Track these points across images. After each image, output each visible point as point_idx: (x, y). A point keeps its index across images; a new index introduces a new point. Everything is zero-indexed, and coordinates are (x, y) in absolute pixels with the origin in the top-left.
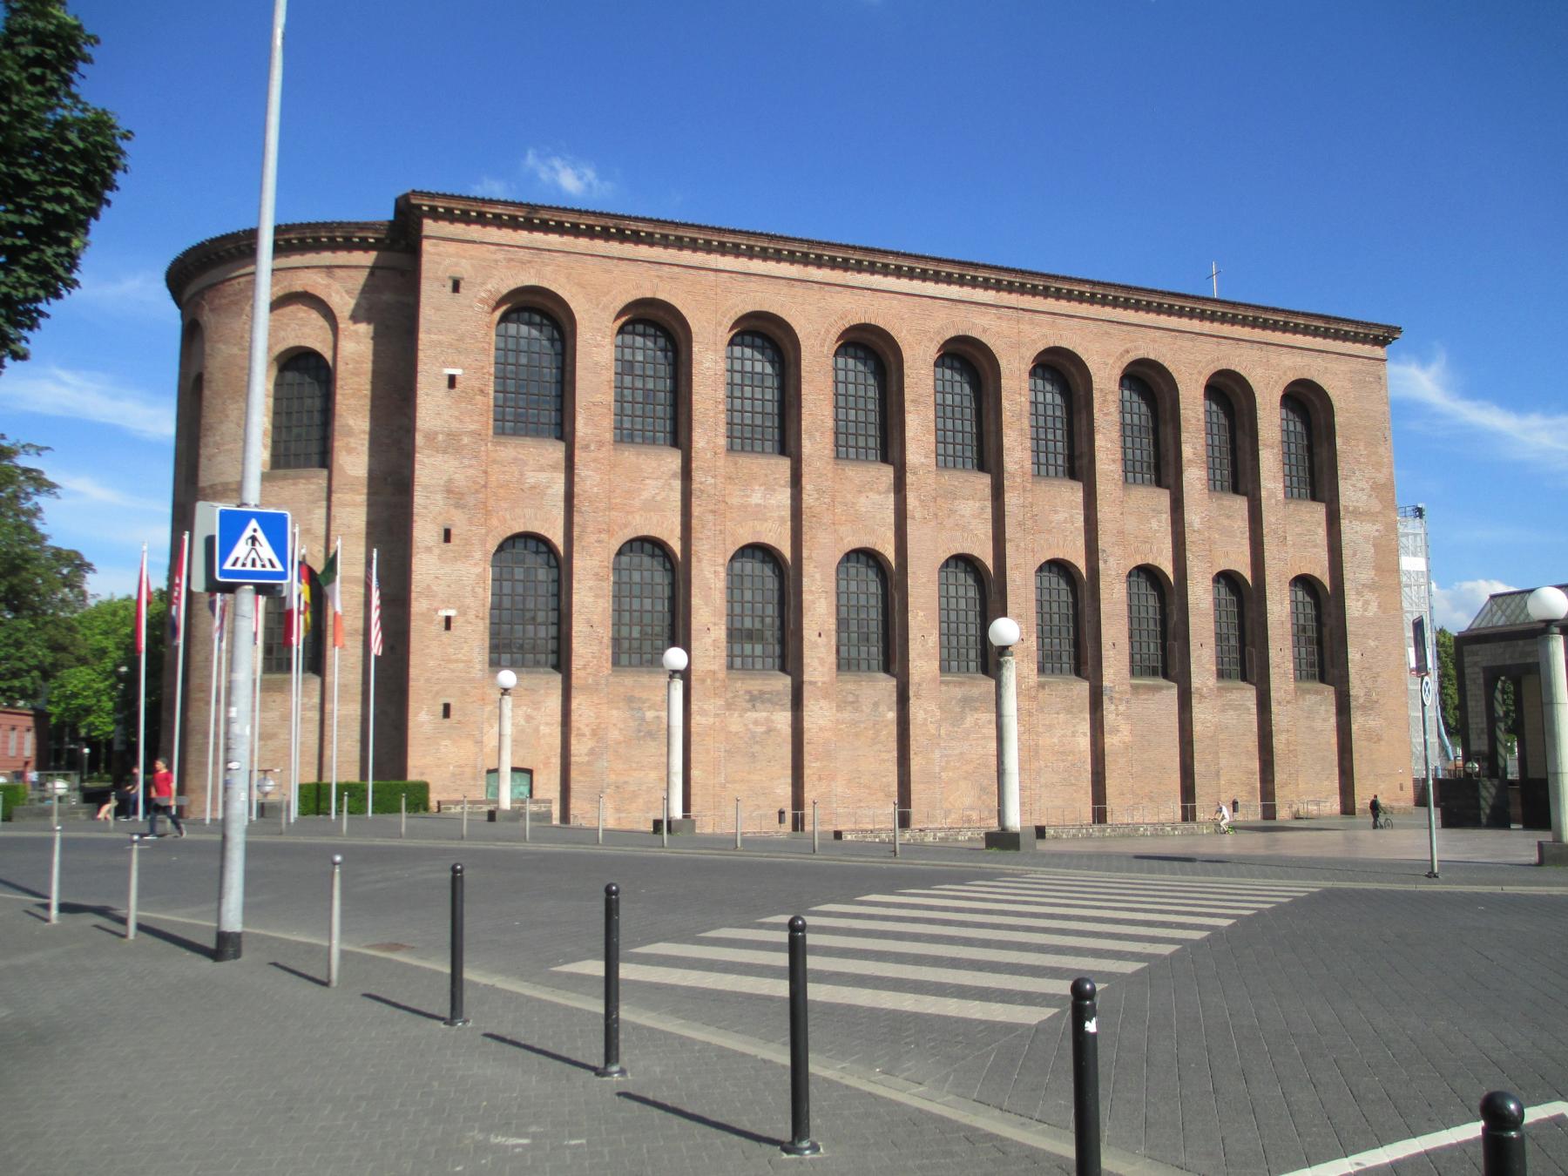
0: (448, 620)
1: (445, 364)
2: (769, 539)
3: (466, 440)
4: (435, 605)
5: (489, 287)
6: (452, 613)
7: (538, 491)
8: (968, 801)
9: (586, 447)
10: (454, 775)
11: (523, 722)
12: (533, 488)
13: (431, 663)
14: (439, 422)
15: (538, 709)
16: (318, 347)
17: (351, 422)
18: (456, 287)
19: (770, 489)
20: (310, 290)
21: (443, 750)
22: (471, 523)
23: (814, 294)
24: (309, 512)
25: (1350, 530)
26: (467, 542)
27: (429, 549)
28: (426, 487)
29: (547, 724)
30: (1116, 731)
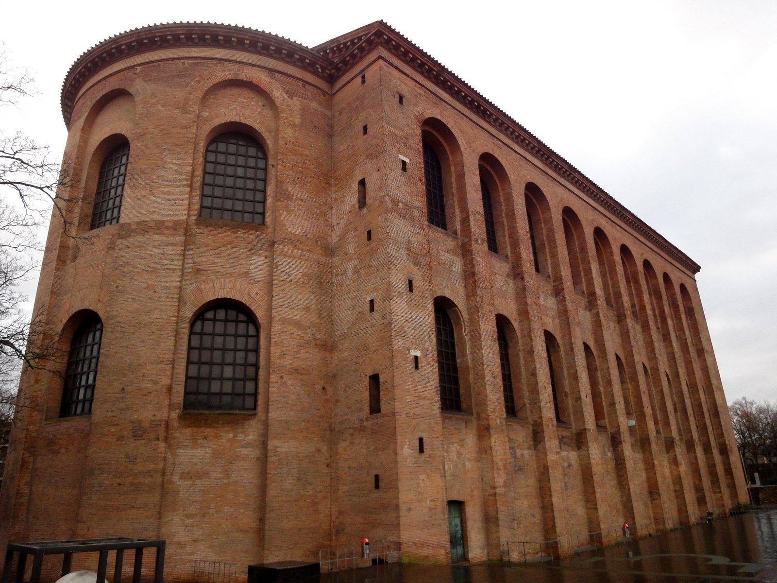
0: (416, 358)
3: (416, 213)
4: (408, 344)
5: (418, 109)
6: (418, 353)
9: (476, 241)
10: (430, 509)
11: (455, 458)
12: (444, 264)
13: (409, 398)
14: (398, 193)
15: (462, 446)
16: (257, 126)
17: (290, 189)
20: (255, 81)
21: (422, 485)
22: (424, 280)
27: (400, 295)
29: (470, 460)
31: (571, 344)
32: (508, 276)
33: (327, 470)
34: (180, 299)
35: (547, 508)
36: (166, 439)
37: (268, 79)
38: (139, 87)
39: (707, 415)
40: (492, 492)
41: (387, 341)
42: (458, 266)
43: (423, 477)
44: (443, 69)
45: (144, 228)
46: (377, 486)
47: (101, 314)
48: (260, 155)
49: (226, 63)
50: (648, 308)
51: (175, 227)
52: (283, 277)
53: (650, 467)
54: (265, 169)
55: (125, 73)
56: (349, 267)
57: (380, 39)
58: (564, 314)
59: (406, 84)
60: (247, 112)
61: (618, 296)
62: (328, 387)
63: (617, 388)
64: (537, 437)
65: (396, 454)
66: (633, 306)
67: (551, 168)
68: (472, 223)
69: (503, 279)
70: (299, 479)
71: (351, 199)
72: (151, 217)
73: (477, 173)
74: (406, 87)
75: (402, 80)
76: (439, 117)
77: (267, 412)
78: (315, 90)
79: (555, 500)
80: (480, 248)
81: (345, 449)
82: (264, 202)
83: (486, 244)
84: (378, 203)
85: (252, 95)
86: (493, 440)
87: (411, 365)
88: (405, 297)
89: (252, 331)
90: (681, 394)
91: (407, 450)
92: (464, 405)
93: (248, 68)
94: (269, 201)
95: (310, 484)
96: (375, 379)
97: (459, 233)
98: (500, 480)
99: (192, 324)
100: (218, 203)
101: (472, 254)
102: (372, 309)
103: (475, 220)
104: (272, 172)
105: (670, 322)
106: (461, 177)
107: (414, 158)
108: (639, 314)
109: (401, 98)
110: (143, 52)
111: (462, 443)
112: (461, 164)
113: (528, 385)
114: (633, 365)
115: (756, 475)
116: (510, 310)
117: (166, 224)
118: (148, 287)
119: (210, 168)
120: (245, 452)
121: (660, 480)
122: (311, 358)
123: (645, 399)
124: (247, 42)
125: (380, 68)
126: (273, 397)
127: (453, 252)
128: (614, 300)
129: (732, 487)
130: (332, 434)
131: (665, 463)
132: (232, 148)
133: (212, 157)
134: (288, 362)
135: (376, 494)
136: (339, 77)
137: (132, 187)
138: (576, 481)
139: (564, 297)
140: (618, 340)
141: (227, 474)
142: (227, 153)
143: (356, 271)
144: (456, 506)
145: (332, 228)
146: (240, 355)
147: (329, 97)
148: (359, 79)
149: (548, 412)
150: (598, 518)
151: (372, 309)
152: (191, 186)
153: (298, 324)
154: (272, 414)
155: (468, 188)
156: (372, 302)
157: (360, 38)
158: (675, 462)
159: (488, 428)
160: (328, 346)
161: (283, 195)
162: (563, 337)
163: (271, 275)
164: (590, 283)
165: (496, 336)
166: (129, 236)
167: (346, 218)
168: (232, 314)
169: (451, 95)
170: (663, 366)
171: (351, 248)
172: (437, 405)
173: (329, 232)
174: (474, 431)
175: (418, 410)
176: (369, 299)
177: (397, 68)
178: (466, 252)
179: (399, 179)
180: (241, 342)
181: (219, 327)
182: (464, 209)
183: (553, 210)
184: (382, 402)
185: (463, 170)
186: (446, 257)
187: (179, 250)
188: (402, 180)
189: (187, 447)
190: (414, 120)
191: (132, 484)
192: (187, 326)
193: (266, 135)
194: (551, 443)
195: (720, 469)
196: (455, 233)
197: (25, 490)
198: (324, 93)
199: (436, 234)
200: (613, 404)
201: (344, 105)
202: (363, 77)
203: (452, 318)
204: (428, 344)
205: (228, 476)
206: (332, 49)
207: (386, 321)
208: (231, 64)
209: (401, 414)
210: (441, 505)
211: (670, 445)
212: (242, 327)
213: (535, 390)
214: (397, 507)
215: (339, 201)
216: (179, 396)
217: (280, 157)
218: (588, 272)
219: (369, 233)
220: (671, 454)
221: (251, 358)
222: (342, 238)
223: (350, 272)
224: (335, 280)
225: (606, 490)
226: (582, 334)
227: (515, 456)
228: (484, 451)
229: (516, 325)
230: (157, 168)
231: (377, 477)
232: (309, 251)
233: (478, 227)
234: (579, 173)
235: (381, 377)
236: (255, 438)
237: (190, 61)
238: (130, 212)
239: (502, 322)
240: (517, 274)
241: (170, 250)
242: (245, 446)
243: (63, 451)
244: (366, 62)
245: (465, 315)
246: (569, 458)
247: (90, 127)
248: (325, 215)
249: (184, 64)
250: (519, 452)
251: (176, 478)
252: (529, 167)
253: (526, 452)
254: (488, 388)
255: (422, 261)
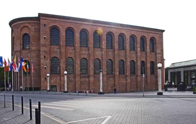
0: (45, 67)
2: (85, 57)
7: (56, 52)
8: (110, 89)
18: (45, 26)
19: (85, 51)
25: (158, 55)
26: (47, 58)
30: (128, 80)
87: (43, 69)
152: (20, 45)
153: (34, 63)
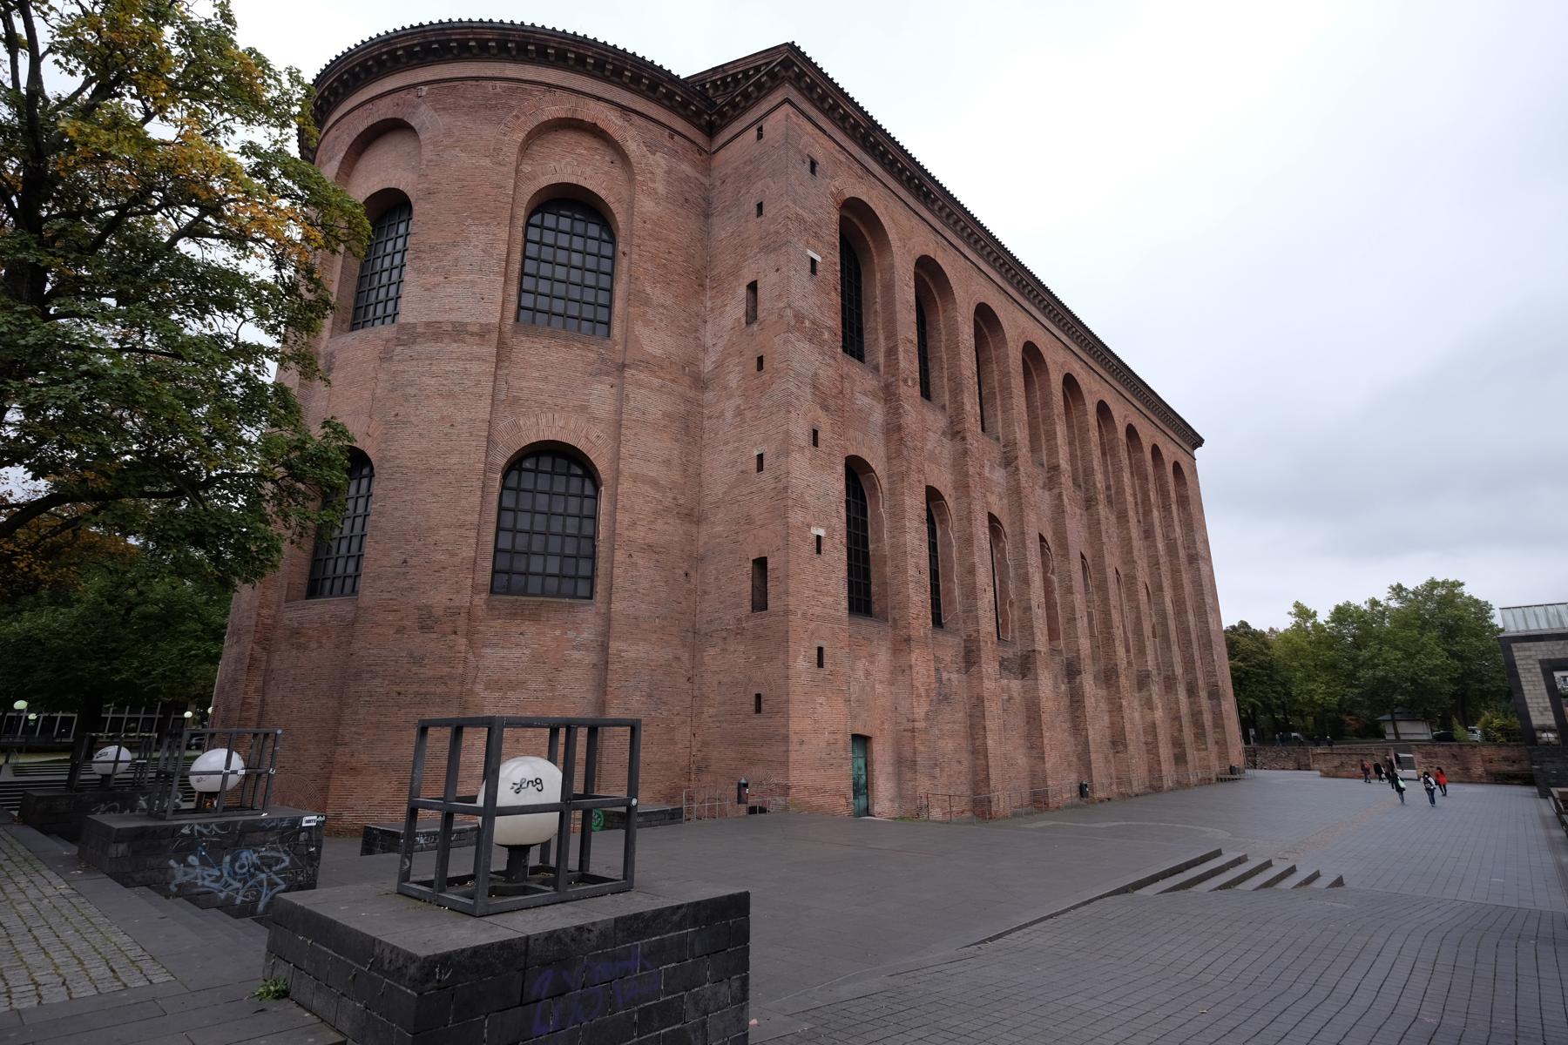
0: (819, 537)
1: (808, 245)
3: (826, 335)
4: (809, 519)
6: (822, 532)
9: (905, 381)
16: (602, 193)
17: (648, 290)
20: (601, 124)
21: (820, 710)
23: (1012, 307)
24: (585, 385)
28: (798, 374)
31: (1023, 533)
32: (944, 433)
33: (688, 685)
34: (490, 440)
35: (978, 752)
36: (469, 635)
37: (619, 122)
38: (423, 117)
39: (1195, 645)
40: (909, 726)
41: (781, 515)
42: (878, 415)
43: (821, 700)
44: (875, 126)
45: (435, 332)
46: (758, 710)
47: (371, 453)
48: (605, 237)
49: (558, 92)
50: (1128, 491)
51: (483, 333)
52: (636, 416)
53: (1116, 708)
54: (612, 258)
55: (402, 94)
56: (729, 407)
57: (786, 71)
58: (1015, 493)
59: (822, 146)
60: (589, 171)
61: (1088, 472)
62: (692, 573)
63: (1078, 598)
64: (970, 657)
65: (788, 667)
66: (1108, 488)
67: (1011, 284)
68: (901, 355)
69: (937, 437)
70: (650, 696)
71: (736, 309)
72: (446, 317)
73: (912, 283)
74: (821, 149)
75: (821, 143)
76: (865, 198)
77: (610, 602)
78: (687, 144)
79: (989, 742)
80: (910, 392)
81: (714, 658)
82: (609, 307)
83: (918, 388)
84: (775, 318)
85: (595, 144)
86: (914, 656)
88: (807, 453)
89: (589, 490)
90: (1164, 616)
91: (802, 663)
92: (875, 608)
93: (592, 103)
94: (618, 305)
95: (665, 703)
96: (761, 564)
97: (882, 368)
98: (921, 710)
99: (505, 477)
100: (543, 303)
101: (898, 400)
102: (760, 468)
103: (906, 351)
104: (623, 264)
105: (1155, 514)
106: (889, 288)
107: (827, 255)
108: (1115, 500)
109: (813, 164)
110: (432, 63)
111: (872, 657)
112: (892, 267)
113: (962, 585)
114: (1101, 570)
115: (1252, 732)
116: (944, 481)
117: (469, 328)
118: (443, 418)
119: (532, 250)
120: (577, 655)
121: (1128, 726)
122: (670, 531)
123: (1115, 615)
124: (591, 61)
125: (782, 119)
126: (618, 582)
127: (874, 396)
128: (1083, 479)
129: (1222, 744)
130: (695, 636)
131: (1136, 704)
132: (565, 223)
133: (534, 234)
134: (639, 534)
135: (757, 720)
136: (722, 127)
137: (418, 271)
138: (1018, 721)
139: (1017, 469)
140: (1084, 534)
141: (551, 683)
142: (557, 230)
143: (739, 413)
144: (861, 741)
145: (705, 350)
146: (572, 525)
147: (706, 157)
148: (753, 132)
149: (987, 626)
150: (1044, 771)
151: (760, 468)
153: (655, 483)
154: (617, 606)
155: (898, 306)
156: (760, 457)
157: (757, 69)
158: (1149, 704)
159: (908, 640)
160: (693, 517)
161: (638, 298)
162: (1012, 524)
163: (619, 412)
164: (1053, 451)
165: (924, 515)
166: (414, 342)
167: (726, 337)
168: (561, 463)
169: (883, 165)
170: (1142, 575)
171: (733, 380)
172: (845, 604)
173: (701, 356)
174: (889, 644)
175: (818, 610)
176: (756, 453)
177: (809, 119)
178: (889, 395)
179: (803, 287)
180: (574, 505)
181: (543, 482)
182: (891, 335)
183: (1011, 344)
184: (770, 597)
185: (892, 279)
186: (863, 401)
187: (489, 367)
188: (810, 286)
189: (496, 645)
190: (831, 200)
191: (417, 694)
192: (499, 476)
193: (614, 207)
194: (989, 667)
195: (1207, 718)
196: (876, 368)
197: (255, 699)
198: (701, 151)
199: (852, 367)
200: (1072, 620)
201: (729, 171)
202: (760, 129)
203: (865, 485)
204: (835, 520)
205: (553, 688)
206: (714, 83)
207: (780, 486)
208: (565, 94)
209: (795, 614)
210: (844, 740)
211: (1142, 681)
212: (575, 483)
213: (971, 593)
214: (786, 739)
215: (717, 312)
216: (485, 577)
217: (636, 241)
218: (1052, 436)
219: (760, 360)
220: (1144, 693)
221: (587, 530)
222: (720, 365)
223: (729, 414)
224: (707, 423)
225: (1056, 734)
226: (1037, 522)
227: (940, 680)
228: (900, 671)
229: (950, 502)
230: (455, 245)
231: (758, 696)
232: (673, 381)
233: (908, 363)
234: (1051, 294)
235: (770, 561)
236: (592, 637)
237: (505, 84)
238: (412, 309)
239: (933, 495)
240: (955, 432)
241: (475, 367)
242: (574, 648)
243: (314, 645)
244: (765, 106)
245: (884, 483)
246: (1009, 689)
247: (349, 176)
248: (697, 331)
249: (494, 88)
250: (945, 676)
251: (479, 688)
252: (982, 280)
253: (954, 676)
254: (911, 586)
255: (831, 402)
